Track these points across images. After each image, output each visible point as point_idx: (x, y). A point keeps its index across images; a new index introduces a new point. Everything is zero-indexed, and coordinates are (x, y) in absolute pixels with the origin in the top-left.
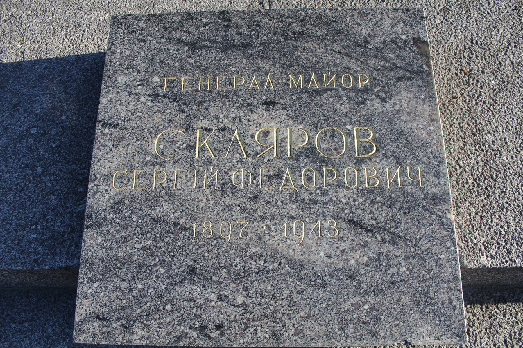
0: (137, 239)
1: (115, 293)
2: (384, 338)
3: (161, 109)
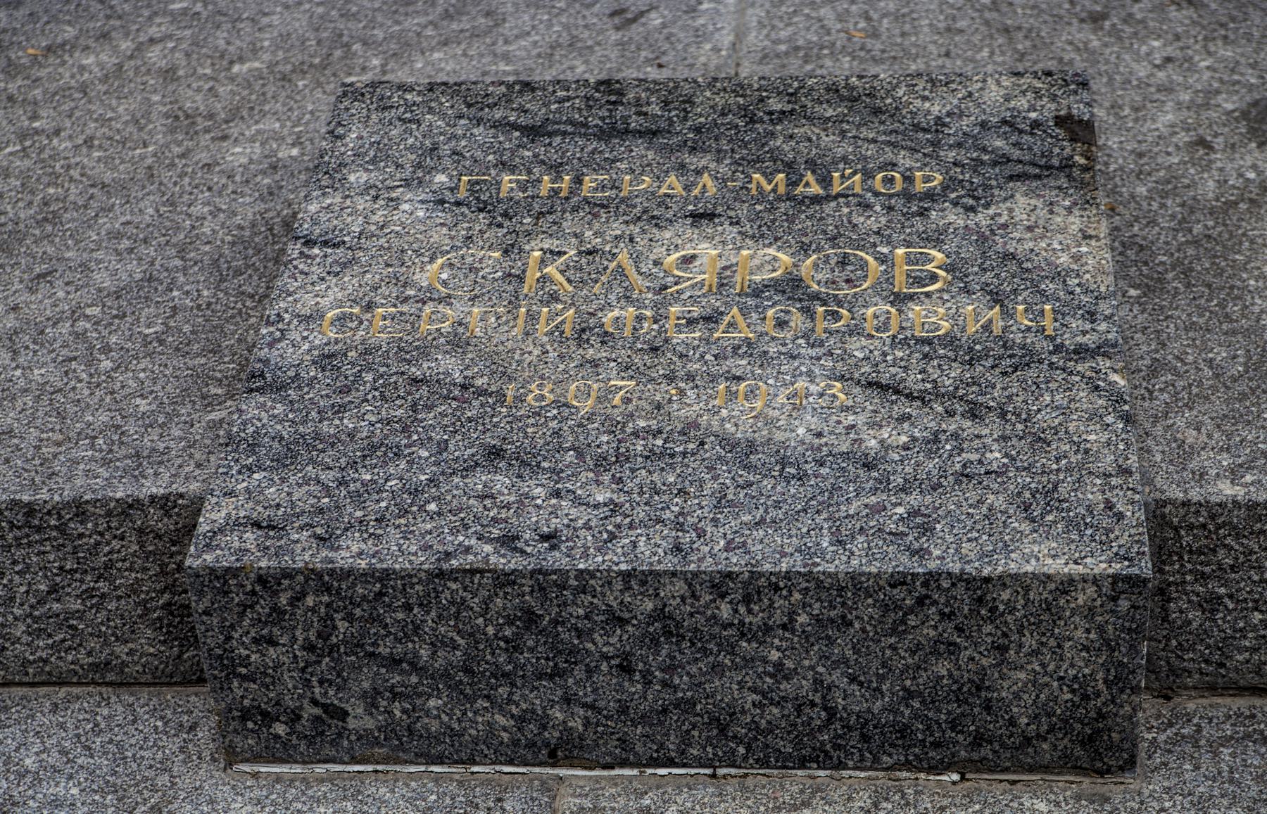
2: (942, 558)
3: (448, 222)
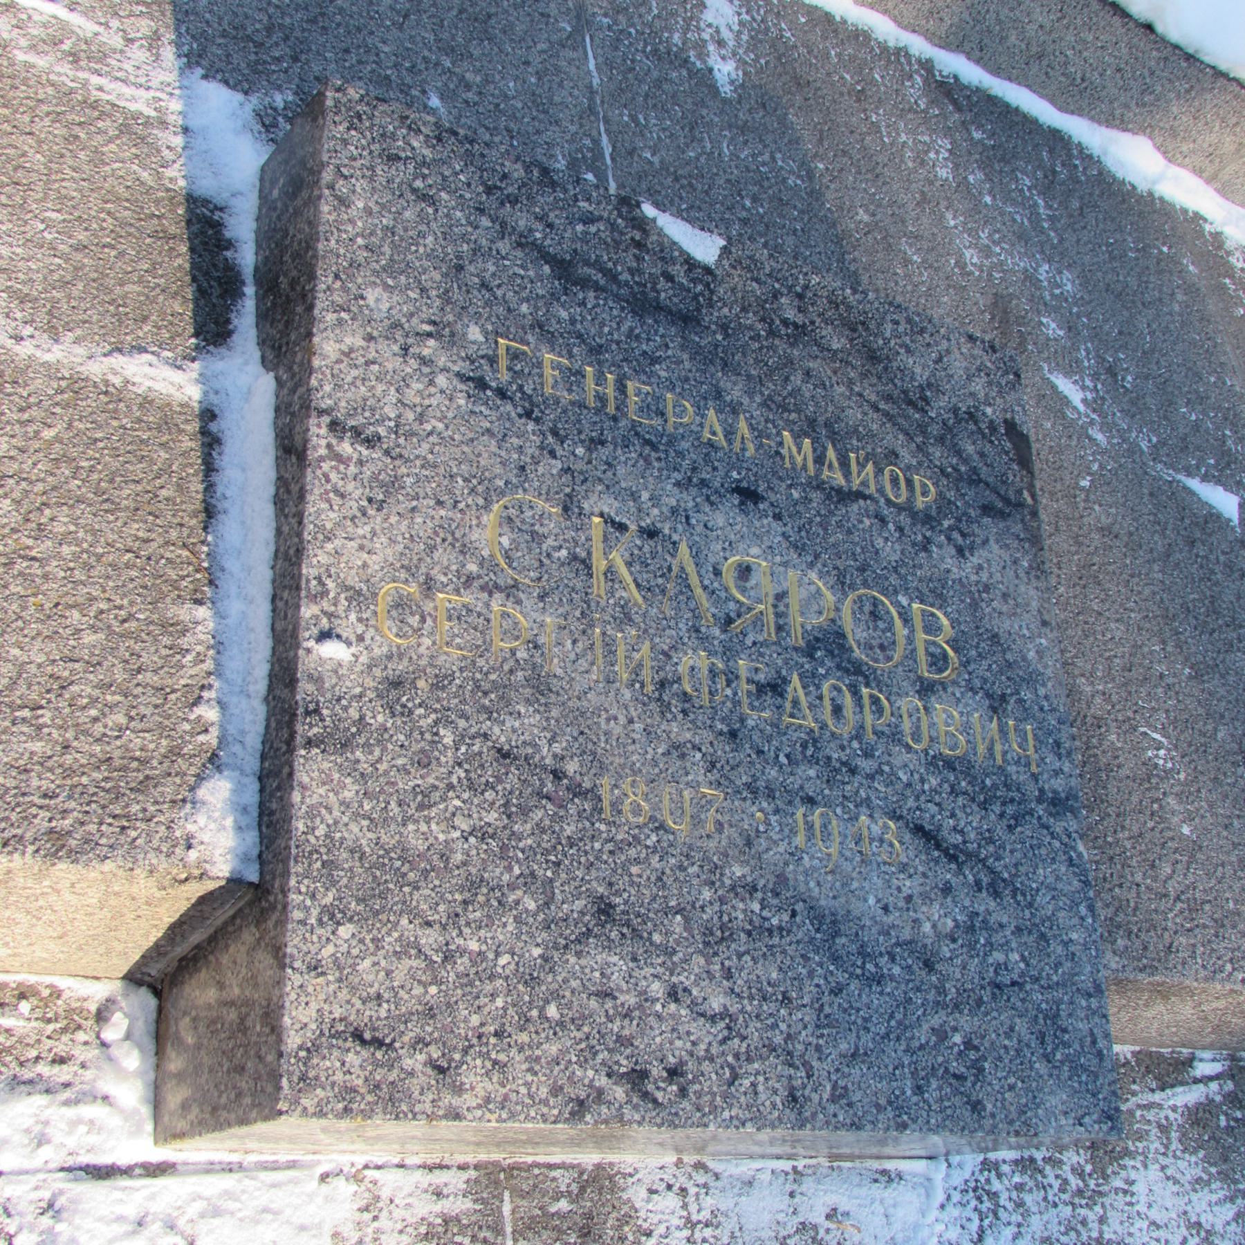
0: (457, 803)
1: (407, 963)
